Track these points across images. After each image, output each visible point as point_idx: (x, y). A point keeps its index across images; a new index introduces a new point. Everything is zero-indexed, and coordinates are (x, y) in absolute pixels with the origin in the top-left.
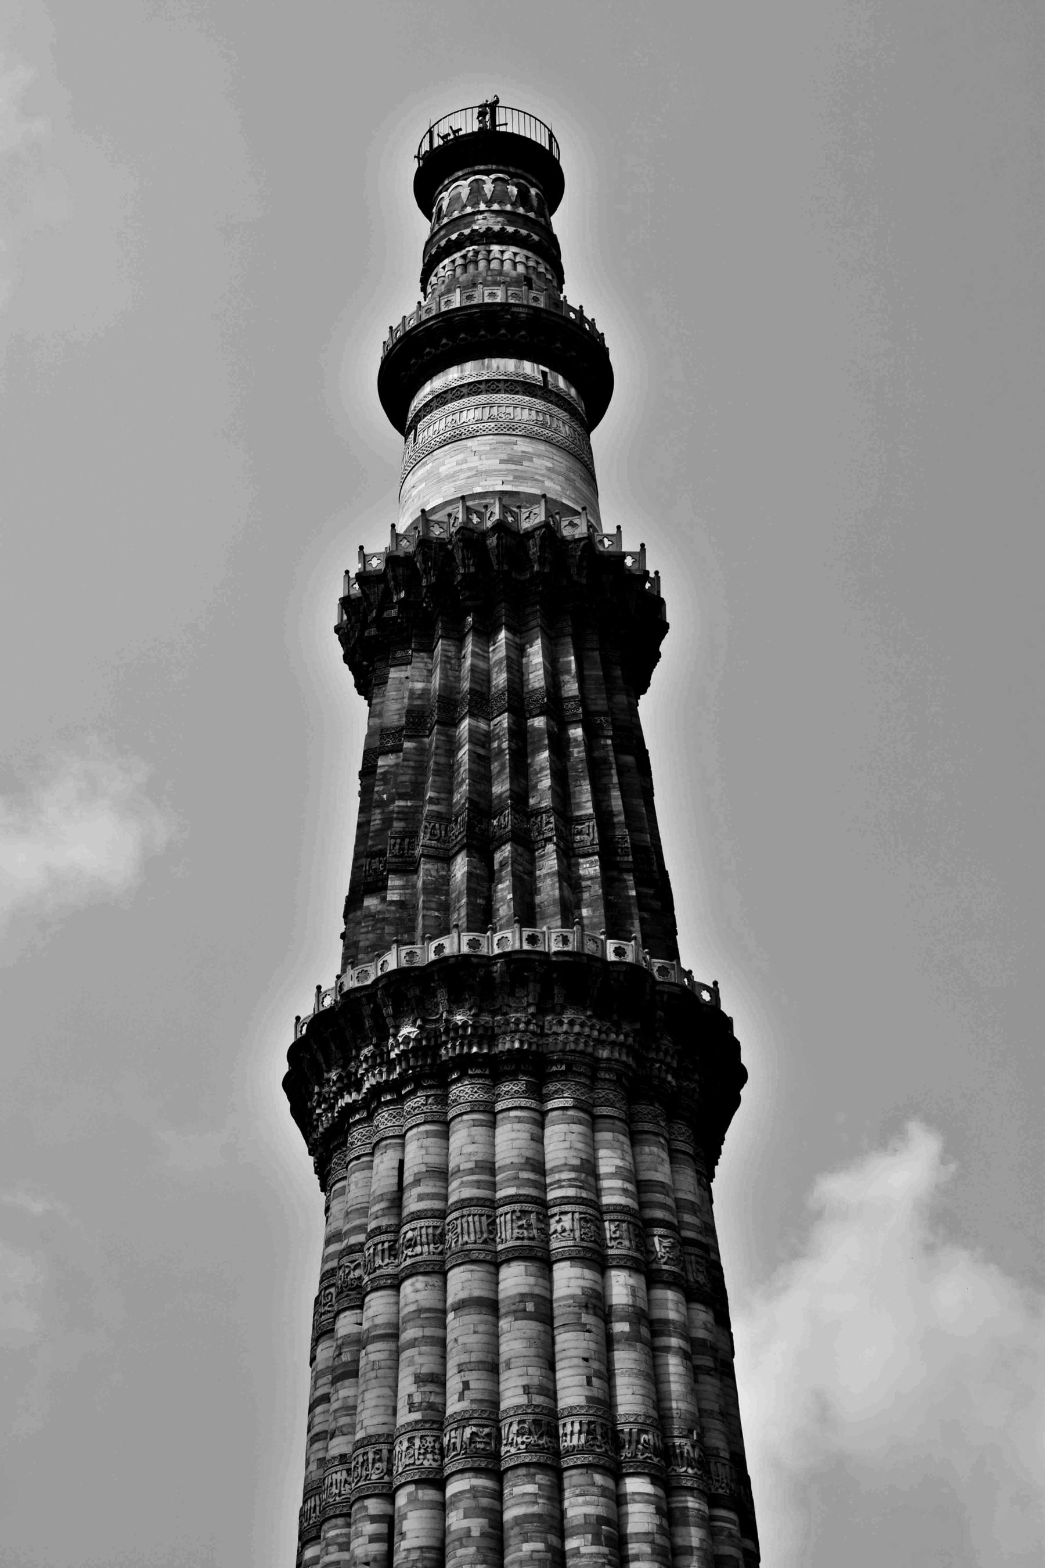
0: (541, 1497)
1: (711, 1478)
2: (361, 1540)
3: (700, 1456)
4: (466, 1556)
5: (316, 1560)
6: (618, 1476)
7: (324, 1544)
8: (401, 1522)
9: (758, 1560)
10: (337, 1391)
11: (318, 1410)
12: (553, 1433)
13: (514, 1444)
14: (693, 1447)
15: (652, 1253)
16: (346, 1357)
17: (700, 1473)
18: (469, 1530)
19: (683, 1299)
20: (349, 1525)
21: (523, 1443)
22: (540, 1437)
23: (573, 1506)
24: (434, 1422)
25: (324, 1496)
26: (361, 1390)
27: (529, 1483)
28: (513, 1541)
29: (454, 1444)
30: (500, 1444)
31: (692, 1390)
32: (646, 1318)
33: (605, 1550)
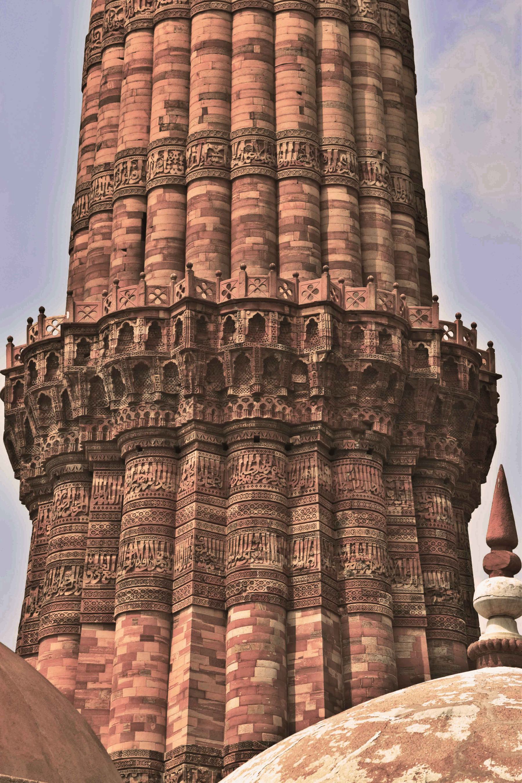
0: (261, 201)
1: (394, 190)
2: (120, 231)
3: (386, 173)
4: (202, 246)
5: (84, 246)
6: (321, 187)
7: (91, 233)
8: (152, 218)
9: (429, 256)
10: (103, 112)
11: (88, 127)
12: (272, 152)
13: (242, 158)
14: (381, 165)
15: (355, 7)
16: (111, 85)
17: (385, 186)
18: (204, 225)
19: (378, 46)
20: (111, 219)
21: (248, 158)
22: (263, 152)
23: (285, 209)
24: (179, 139)
25: (92, 196)
26: (121, 113)
27: (252, 190)
28: (238, 235)
29: (195, 157)
30: (231, 158)
31: (382, 119)
32: (347, 60)
33: (310, 244)
